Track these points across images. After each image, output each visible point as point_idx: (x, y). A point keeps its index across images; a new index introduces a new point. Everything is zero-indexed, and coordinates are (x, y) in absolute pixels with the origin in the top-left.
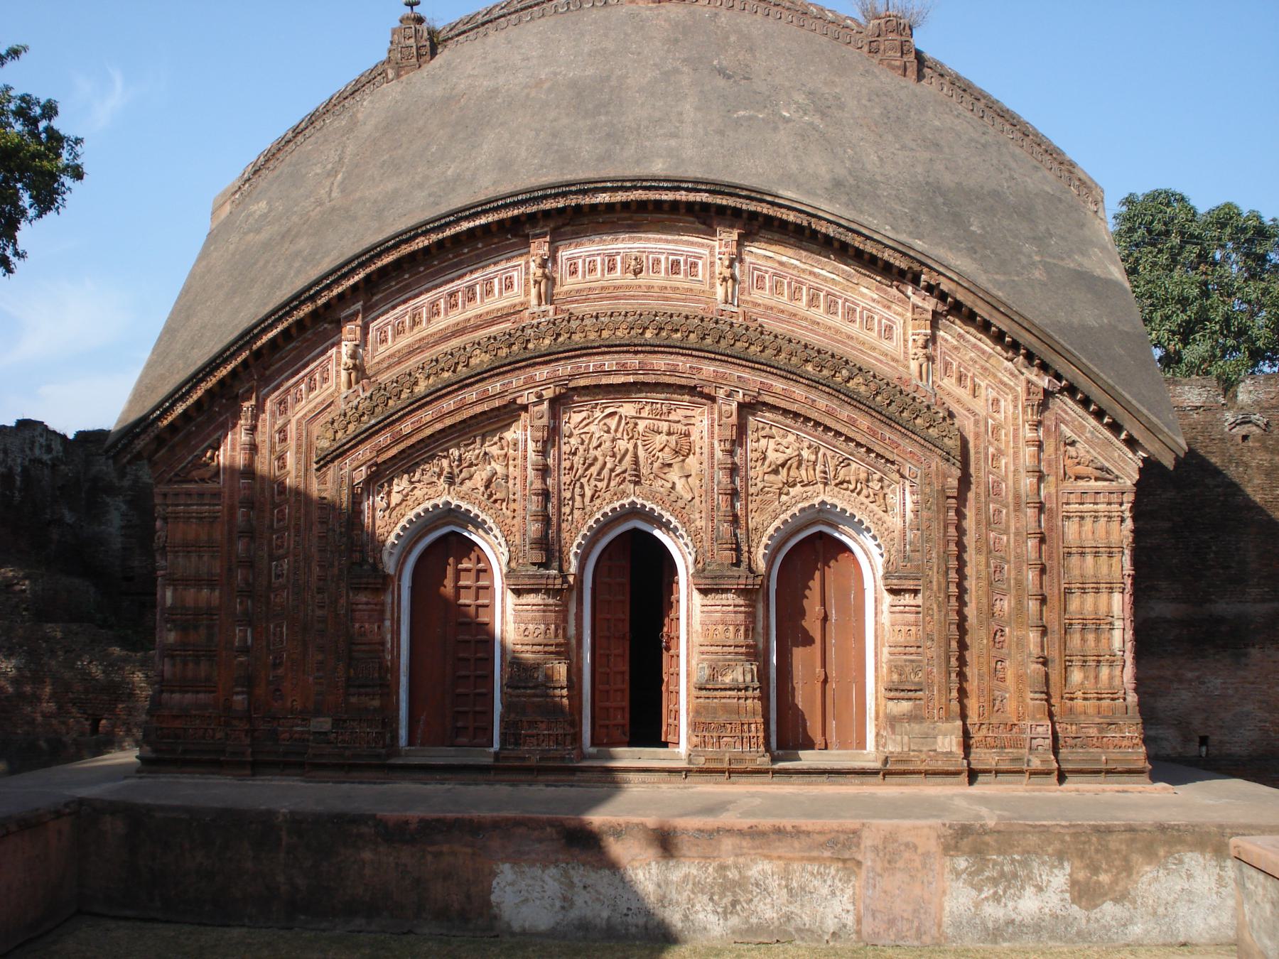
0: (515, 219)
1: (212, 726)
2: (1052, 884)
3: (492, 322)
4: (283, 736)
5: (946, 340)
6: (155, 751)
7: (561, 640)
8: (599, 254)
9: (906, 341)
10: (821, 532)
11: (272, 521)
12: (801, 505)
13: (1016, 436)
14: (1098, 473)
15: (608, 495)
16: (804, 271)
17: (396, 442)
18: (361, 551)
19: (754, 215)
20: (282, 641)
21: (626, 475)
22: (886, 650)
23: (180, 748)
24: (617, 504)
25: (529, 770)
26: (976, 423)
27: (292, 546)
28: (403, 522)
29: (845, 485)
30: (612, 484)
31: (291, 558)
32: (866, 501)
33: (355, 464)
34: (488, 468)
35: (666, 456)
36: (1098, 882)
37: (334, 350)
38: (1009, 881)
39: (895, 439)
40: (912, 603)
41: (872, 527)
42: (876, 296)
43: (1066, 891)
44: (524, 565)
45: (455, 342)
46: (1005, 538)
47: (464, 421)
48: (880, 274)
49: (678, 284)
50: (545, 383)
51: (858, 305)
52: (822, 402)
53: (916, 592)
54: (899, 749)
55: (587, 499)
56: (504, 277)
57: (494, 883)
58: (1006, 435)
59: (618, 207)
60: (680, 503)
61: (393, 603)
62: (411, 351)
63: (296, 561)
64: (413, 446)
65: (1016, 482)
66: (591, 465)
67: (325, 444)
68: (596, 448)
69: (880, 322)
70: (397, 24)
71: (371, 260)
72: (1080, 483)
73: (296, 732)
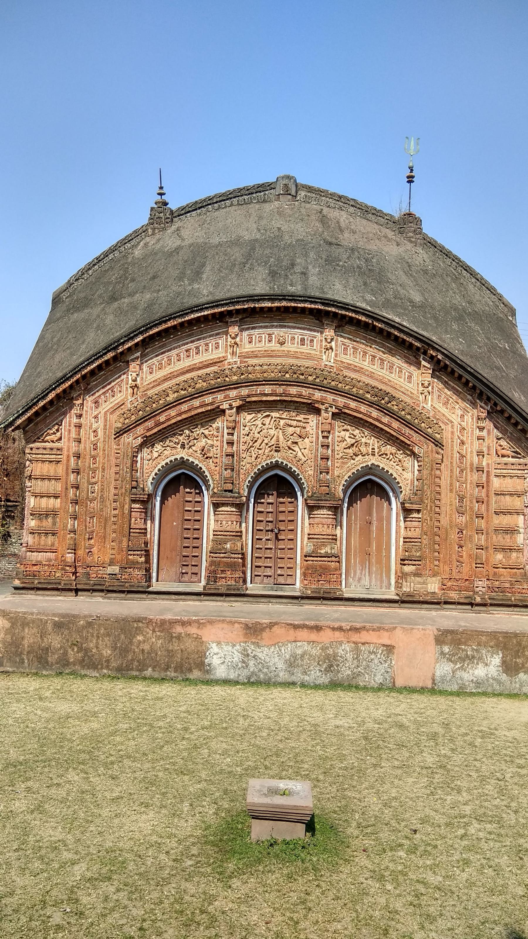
0: (221, 313)
2: (493, 663)
3: (207, 366)
4: (92, 576)
7: (238, 529)
10: (370, 479)
12: (362, 465)
13: (472, 433)
14: (513, 454)
15: (264, 457)
17: (157, 424)
18: (137, 481)
19: (344, 317)
21: (274, 447)
22: (402, 540)
23: (36, 582)
24: (269, 462)
25: (221, 595)
26: (452, 426)
28: (159, 467)
29: (384, 456)
30: (266, 451)
32: (395, 464)
33: (136, 435)
34: (204, 440)
35: (296, 438)
36: (516, 662)
37: (125, 376)
38: (470, 660)
41: (397, 477)
43: (500, 666)
44: (221, 491)
45: (188, 376)
46: (464, 485)
47: (192, 416)
48: (407, 349)
49: (303, 351)
50: (234, 399)
51: (394, 365)
52: (375, 414)
53: (418, 511)
55: (253, 459)
57: (207, 654)
59: (275, 309)
62: (166, 379)
64: (165, 428)
66: (256, 441)
67: (120, 425)
68: (259, 433)
71: (146, 331)
72: (505, 459)
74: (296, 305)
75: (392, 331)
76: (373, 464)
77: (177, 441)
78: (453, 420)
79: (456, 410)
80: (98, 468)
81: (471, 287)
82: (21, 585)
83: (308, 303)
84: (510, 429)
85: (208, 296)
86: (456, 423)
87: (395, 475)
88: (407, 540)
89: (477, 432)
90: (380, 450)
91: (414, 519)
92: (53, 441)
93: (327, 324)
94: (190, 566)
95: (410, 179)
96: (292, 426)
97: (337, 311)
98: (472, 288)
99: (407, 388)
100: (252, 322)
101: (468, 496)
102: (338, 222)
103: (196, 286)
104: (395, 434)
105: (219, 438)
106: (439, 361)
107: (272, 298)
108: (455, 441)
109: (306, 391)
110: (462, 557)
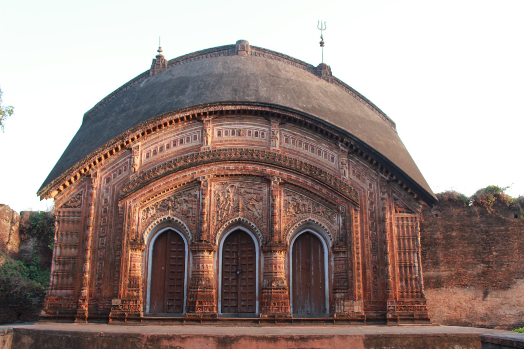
1: (72, 303)
5: (353, 163)
6: (46, 313)
9: (339, 163)
11: (101, 223)
12: (302, 221)
14: (406, 210)
16: (302, 137)
19: (284, 117)
20: (102, 269)
22: (333, 275)
23: (58, 312)
27: (108, 232)
31: (108, 237)
40: (343, 256)
42: (327, 147)
48: (329, 139)
51: (321, 150)
54: (340, 312)
56: (193, 135)
60: (257, 219)
61: (146, 256)
63: (109, 238)
65: (379, 213)
70: (155, 58)
73: (105, 306)
74: (251, 108)
75: (319, 126)
76: (310, 220)
77: (165, 205)
78: (364, 187)
82: (46, 315)
83: (260, 107)
84: (403, 193)
85: (189, 103)
86: (366, 189)
87: (326, 227)
88: (337, 274)
89: (381, 195)
90: (315, 210)
91: (341, 259)
92: (75, 207)
93: (273, 122)
94: (175, 301)
95: (322, 44)
96: (250, 193)
97: (280, 113)
99: (331, 165)
100: (220, 121)
101: (378, 240)
102: (277, 66)
103: (181, 97)
104: (324, 197)
105: (196, 203)
106: (351, 147)
107: (233, 103)
109: (260, 168)
110: (376, 285)
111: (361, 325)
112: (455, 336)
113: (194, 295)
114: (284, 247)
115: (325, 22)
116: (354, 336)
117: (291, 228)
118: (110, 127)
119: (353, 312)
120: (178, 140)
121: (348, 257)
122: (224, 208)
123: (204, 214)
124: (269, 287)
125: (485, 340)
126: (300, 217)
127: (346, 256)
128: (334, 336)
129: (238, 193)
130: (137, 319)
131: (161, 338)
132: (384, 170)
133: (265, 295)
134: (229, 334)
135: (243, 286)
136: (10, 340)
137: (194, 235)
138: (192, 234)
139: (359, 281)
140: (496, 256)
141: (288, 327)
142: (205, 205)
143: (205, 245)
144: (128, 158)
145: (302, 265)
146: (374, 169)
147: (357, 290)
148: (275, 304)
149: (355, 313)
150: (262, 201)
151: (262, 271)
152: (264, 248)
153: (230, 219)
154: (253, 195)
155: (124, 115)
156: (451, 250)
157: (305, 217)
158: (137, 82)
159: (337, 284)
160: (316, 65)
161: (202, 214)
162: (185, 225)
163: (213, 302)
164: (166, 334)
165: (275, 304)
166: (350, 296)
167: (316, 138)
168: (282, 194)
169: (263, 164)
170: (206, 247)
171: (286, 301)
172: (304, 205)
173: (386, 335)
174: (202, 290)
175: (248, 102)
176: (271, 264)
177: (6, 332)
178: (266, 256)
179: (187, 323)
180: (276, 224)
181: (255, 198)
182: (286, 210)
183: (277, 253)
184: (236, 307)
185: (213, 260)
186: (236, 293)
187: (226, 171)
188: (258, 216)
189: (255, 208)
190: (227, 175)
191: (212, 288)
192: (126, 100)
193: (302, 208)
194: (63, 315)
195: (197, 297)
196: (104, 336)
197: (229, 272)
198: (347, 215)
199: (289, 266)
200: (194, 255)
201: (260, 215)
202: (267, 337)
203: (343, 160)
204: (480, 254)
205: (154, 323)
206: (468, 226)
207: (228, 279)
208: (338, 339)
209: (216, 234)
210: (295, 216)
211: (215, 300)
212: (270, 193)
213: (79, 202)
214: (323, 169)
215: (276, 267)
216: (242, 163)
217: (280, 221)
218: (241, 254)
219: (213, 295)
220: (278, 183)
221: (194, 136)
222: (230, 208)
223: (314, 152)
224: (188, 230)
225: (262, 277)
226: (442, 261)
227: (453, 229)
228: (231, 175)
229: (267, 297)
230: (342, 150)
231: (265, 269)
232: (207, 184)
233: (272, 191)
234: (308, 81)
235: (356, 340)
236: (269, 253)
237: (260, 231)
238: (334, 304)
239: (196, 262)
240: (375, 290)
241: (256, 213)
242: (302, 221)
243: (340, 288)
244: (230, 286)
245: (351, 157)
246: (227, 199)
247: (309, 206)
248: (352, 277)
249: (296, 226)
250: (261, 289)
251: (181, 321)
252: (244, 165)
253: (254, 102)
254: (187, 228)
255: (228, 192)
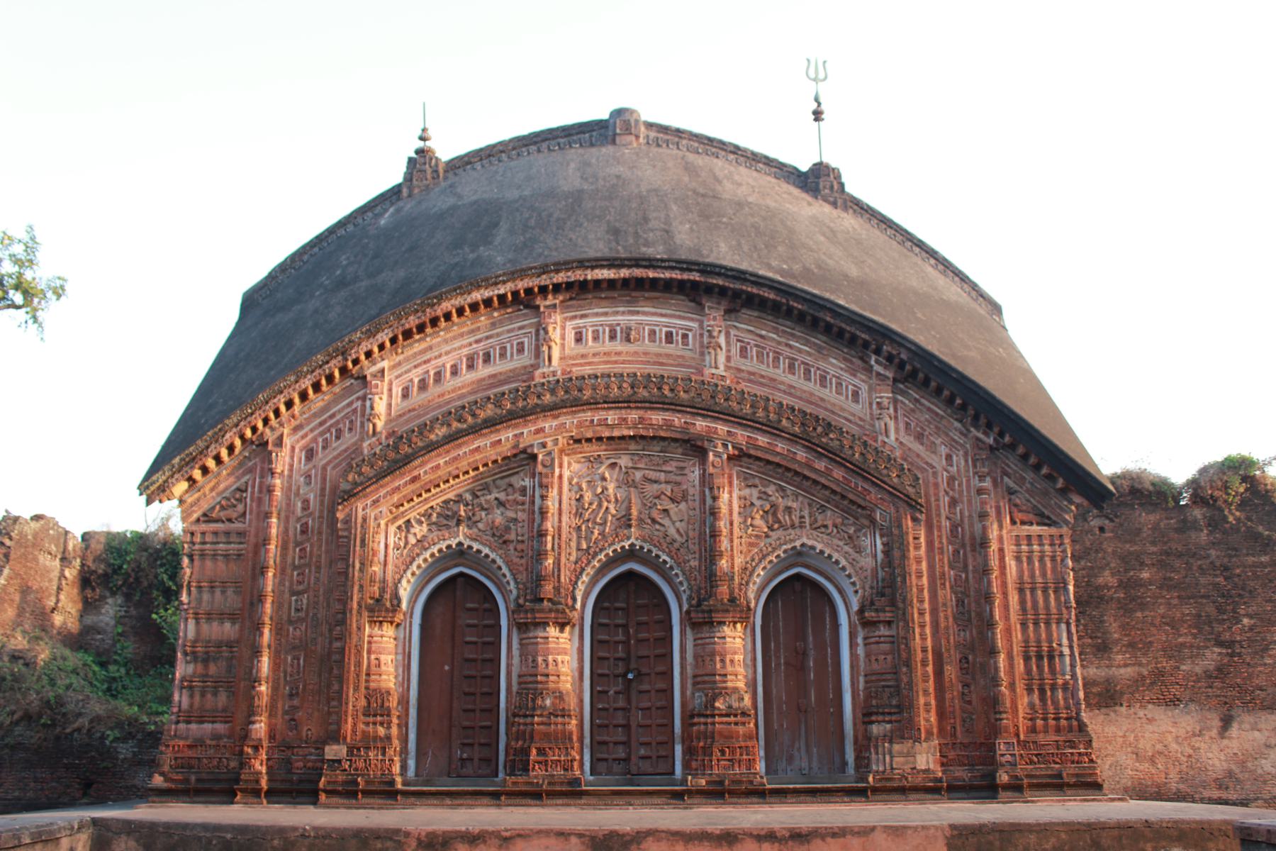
5: (904, 403)
6: (166, 780)
8: (602, 325)
9: (871, 404)
11: (294, 558)
12: (785, 547)
14: (1038, 519)
16: (779, 343)
19: (737, 294)
20: (298, 672)
22: (862, 679)
23: (193, 778)
27: (312, 582)
31: (311, 593)
39: (866, 486)
40: (887, 633)
42: (843, 366)
48: (847, 347)
51: (828, 373)
54: (881, 769)
56: (515, 343)
58: (959, 485)
60: (677, 545)
61: (405, 638)
65: (971, 525)
69: (847, 387)
70: (414, 155)
72: (1027, 527)
73: (309, 761)
74: (656, 275)
75: (821, 315)
76: (803, 545)
77: (449, 513)
78: (934, 464)
79: (938, 448)
80: (309, 565)
81: (930, 269)
82: (165, 785)
83: (678, 272)
84: (1029, 476)
85: (504, 264)
86: (939, 468)
88: (873, 678)
89: (976, 482)
90: (816, 521)
91: (882, 639)
92: (230, 520)
93: (710, 308)
94: (476, 747)
95: (818, 115)
96: (656, 482)
97: (727, 284)
98: (929, 269)
99: (852, 410)
100: (581, 307)
101: (972, 593)
102: (711, 170)
104: (838, 490)
105: (526, 506)
106: (901, 365)
107: (613, 263)
108: (942, 499)
110: (969, 703)
111: (935, 801)
112: (1169, 825)
113: (524, 732)
114: (742, 611)
115: (825, 62)
116: (923, 827)
117: (757, 565)
118: (310, 324)
119: (915, 768)
120: (478, 355)
121: (898, 633)
122: (595, 518)
123: (546, 535)
124: (708, 710)
125: (1251, 835)
126: (779, 539)
127: (893, 632)
128: (873, 829)
129: (627, 482)
130: (387, 793)
131: (452, 838)
132: (983, 420)
133: (699, 731)
134: (617, 828)
135: (641, 709)
136: (84, 846)
137: (521, 586)
138: (516, 582)
139: (926, 693)
140: (1251, 629)
141: (756, 808)
142: (547, 512)
143: (551, 611)
144: (358, 399)
145: (785, 657)
146: (956, 420)
147: (923, 714)
148: (723, 752)
149: (918, 772)
150: (686, 501)
151: (689, 671)
152: (693, 615)
153: (610, 546)
154: (663, 486)
155: (343, 294)
156: (1139, 614)
157: (792, 537)
158: (370, 214)
159: (874, 702)
160: (804, 167)
161: (542, 534)
162: (500, 562)
163: (573, 748)
164: (463, 829)
165: (723, 752)
166: (906, 730)
167: (814, 343)
168: (735, 482)
169: (688, 409)
170: (553, 615)
171: (749, 744)
172: (788, 510)
173: (1002, 824)
174: (544, 719)
175: (649, 260)
176: (713, 654)
177: (76, 827)
178: (699, 636)
179: (509, 802)
180: (721, 555)
181: (669, 494)
182: (745, 521)
183: (725, 628)
184: (627, 760)
185: (568, 647)
186: (627, 727)
187: (599, 428)
188: (677, 537)
189: (671, 519)
190: (600, 439)
191: (569, 716)
192: (348, 258)
193: (784, 516)
194: (207, 786)
195: (532, 738)
196: (312, 834)
197: (607, 675)
198: (895, 531)
199: (754, 659)
200: (524, 636)
201: (681, 536)
202: (712, 833)
203: (881, 397)
204: (1210, 623)
205: (554, 802)
206: (1180, 555)
207: (607, 692)
208: (885, 835)
209: (576, 583)
210: (767, 536)
211: (576, 745)
212: (707, 481)
213: (240, 507)
214: (836, 421)
215: (722, 661)
216: (637, 408)
217: (732, 550)
218: (637, 632)
219: (571, 733)
220: (725, 456)
221: (518, 344)
222: (610, 518)
223: (809, 380)
224: (508, 574)
225: (689, 686)
226: (1117, 641)
227: (1142, 564)
228: (611, 438)
229: (705, 735)
230: (878, 374)
231: (696, 666)
232: (553, 460)
233: (711, 475)
234: (788, 205)
235: (927, 837)
236: (706, 628)
237: (684, 574)
238: (868, 749)
239: (529, 653)
240: (965, 715)
241: (672, 531)
242: (785, 547)
243: (881, 710)
244: (611, 710)
245: (901, 390)
246: (601, 497)
247: (801, 511)
248: (910, 684)
249: (771, 562)
250: (689, 717)
251: (495, 795)
252: (641, 412)
253: (663, 260)
254: (505, 570)
255: (604, 479)
